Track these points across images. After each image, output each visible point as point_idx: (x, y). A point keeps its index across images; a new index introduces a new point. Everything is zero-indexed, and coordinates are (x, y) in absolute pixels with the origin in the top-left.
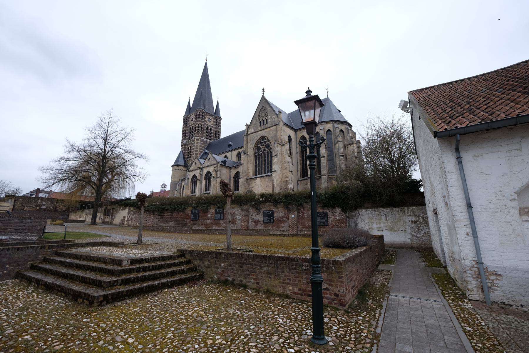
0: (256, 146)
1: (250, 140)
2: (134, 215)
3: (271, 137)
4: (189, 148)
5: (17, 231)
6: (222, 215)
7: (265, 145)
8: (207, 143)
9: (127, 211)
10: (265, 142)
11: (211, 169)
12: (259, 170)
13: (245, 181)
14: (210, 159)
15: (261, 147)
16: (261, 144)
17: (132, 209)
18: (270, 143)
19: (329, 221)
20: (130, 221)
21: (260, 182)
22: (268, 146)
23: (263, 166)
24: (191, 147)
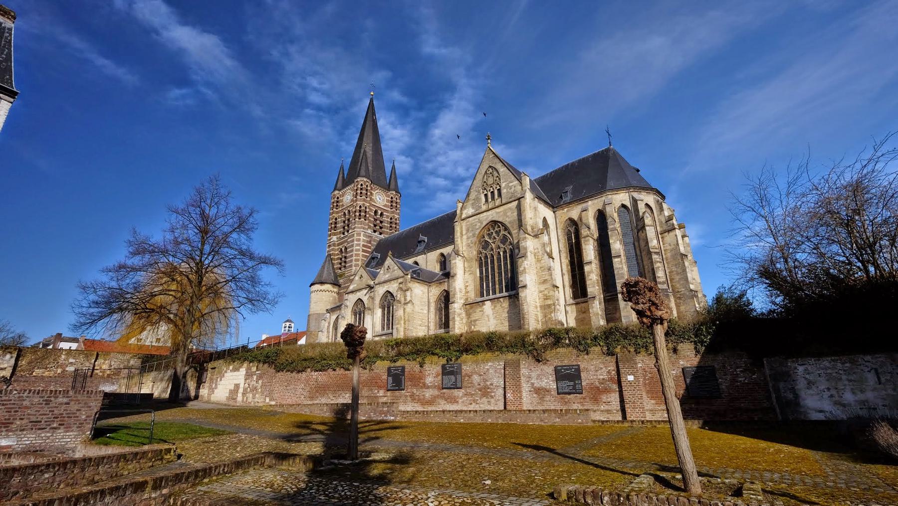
0: (480, 241)
1: (468, 230)
2: (260, 382)
3: (510, 222)
4: (341, 249)
5: (36, 426)
6: (459, 377)
8: (374, 241)
9: (244, 372)
10: (498, 233)
11: (393, 287)
12: (488, 286)
13: (461, 309)
14: (391, 267)
16: (490, 235)
17: (254, 369)
18: (509, 233)
19: (720, 387)
20: (251, 395)
21: (492, 309)
23: (497, 279)
24: (346, 248)
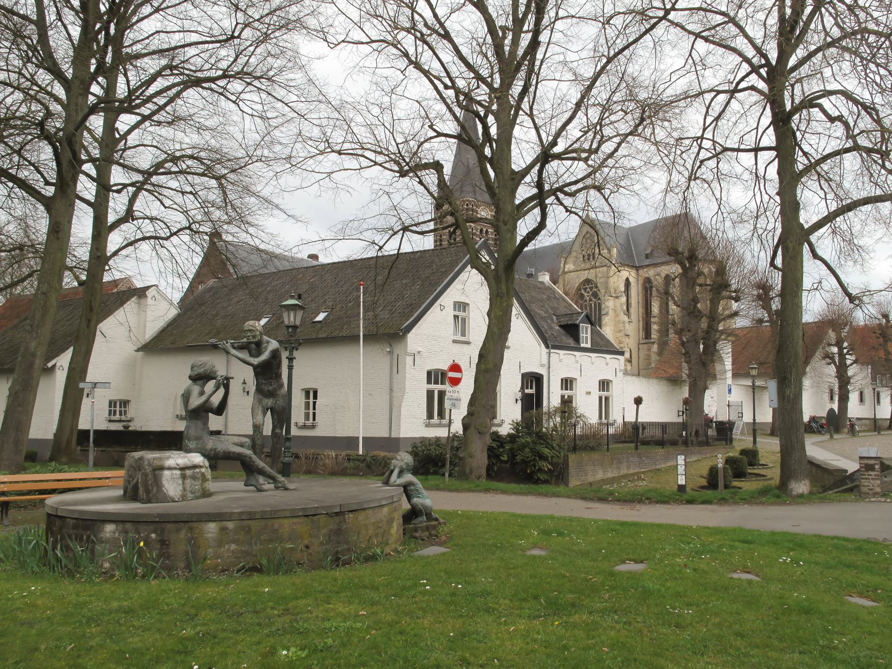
7: (591, 293)
10: (591, 288)
15: (586, 294)
16: (585, 289)
22: (595, 295)
